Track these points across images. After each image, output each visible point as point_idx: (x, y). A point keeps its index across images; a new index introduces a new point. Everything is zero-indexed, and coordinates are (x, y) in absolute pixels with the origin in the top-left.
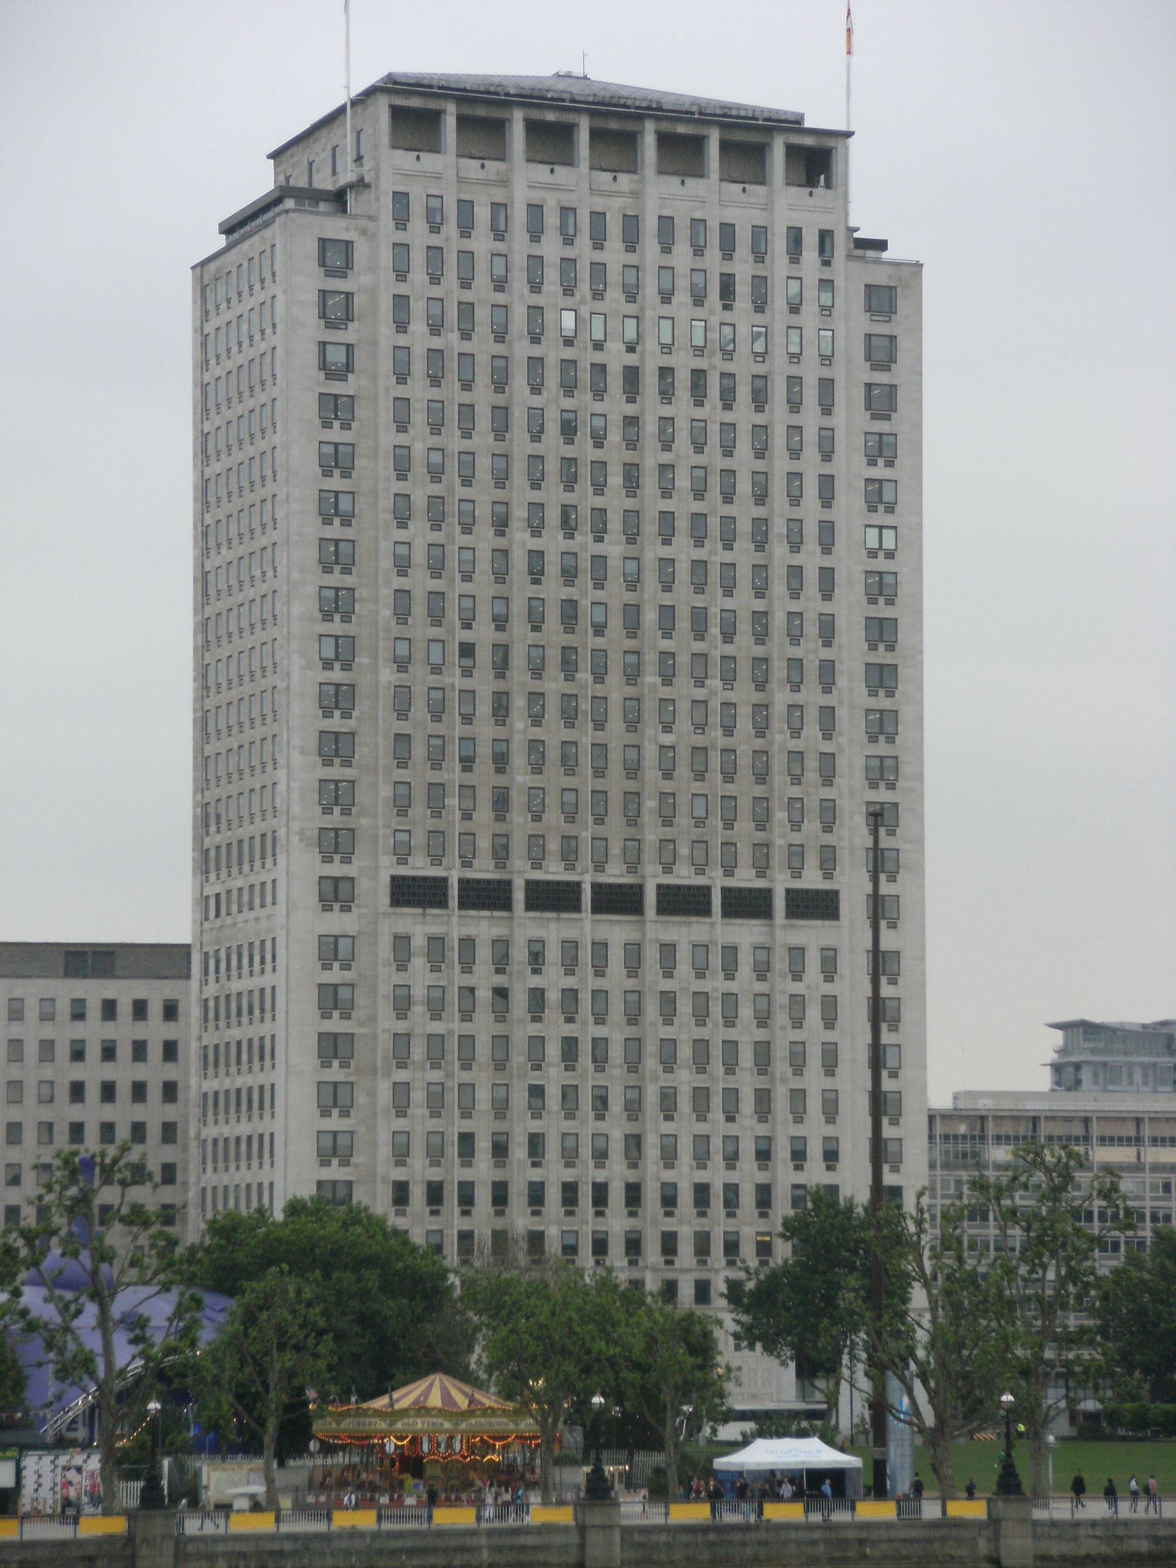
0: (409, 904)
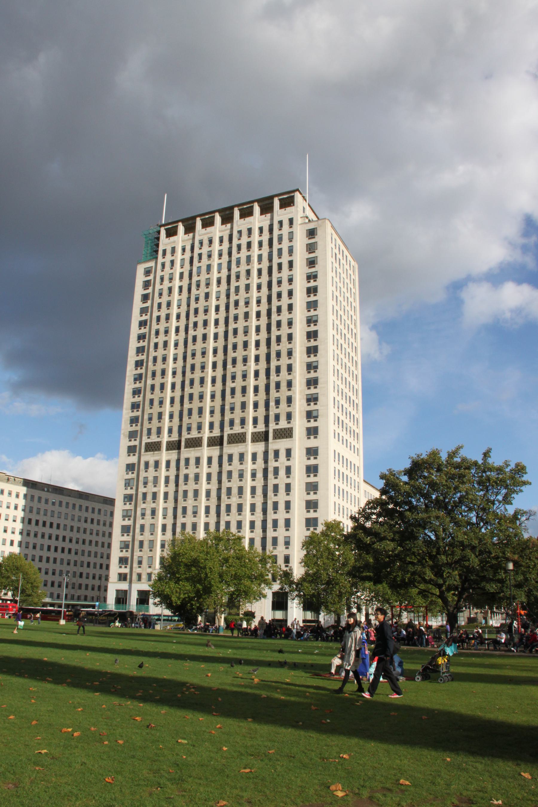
0: (150, 451)
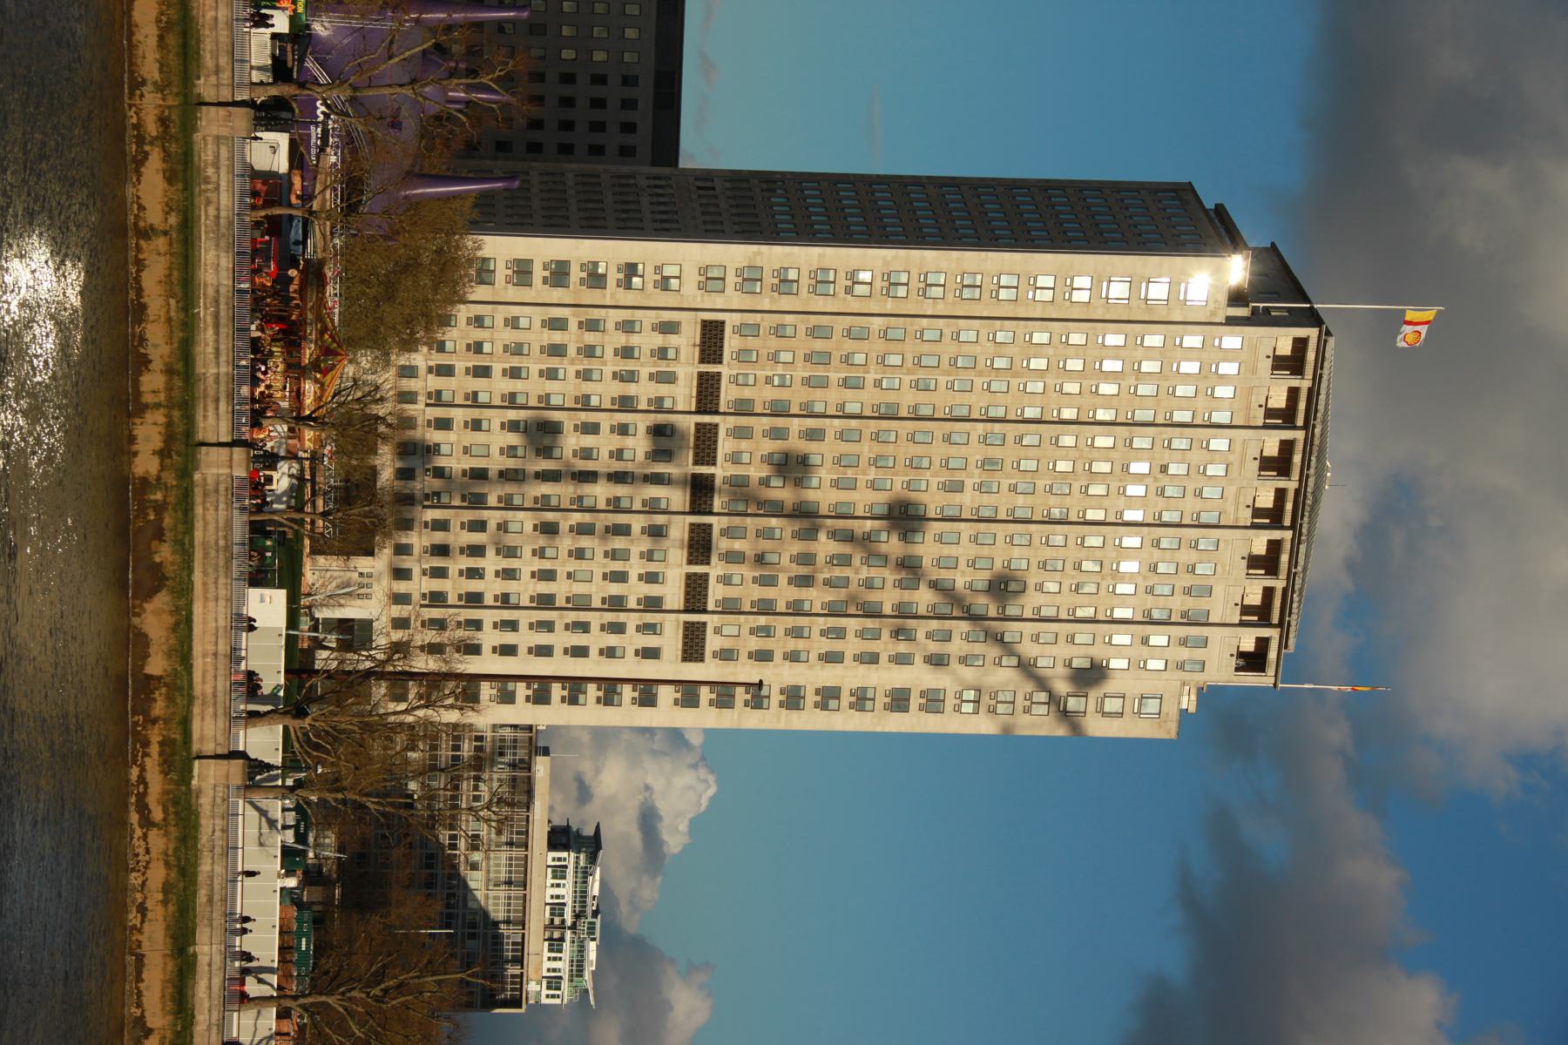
0: (703, 335)
